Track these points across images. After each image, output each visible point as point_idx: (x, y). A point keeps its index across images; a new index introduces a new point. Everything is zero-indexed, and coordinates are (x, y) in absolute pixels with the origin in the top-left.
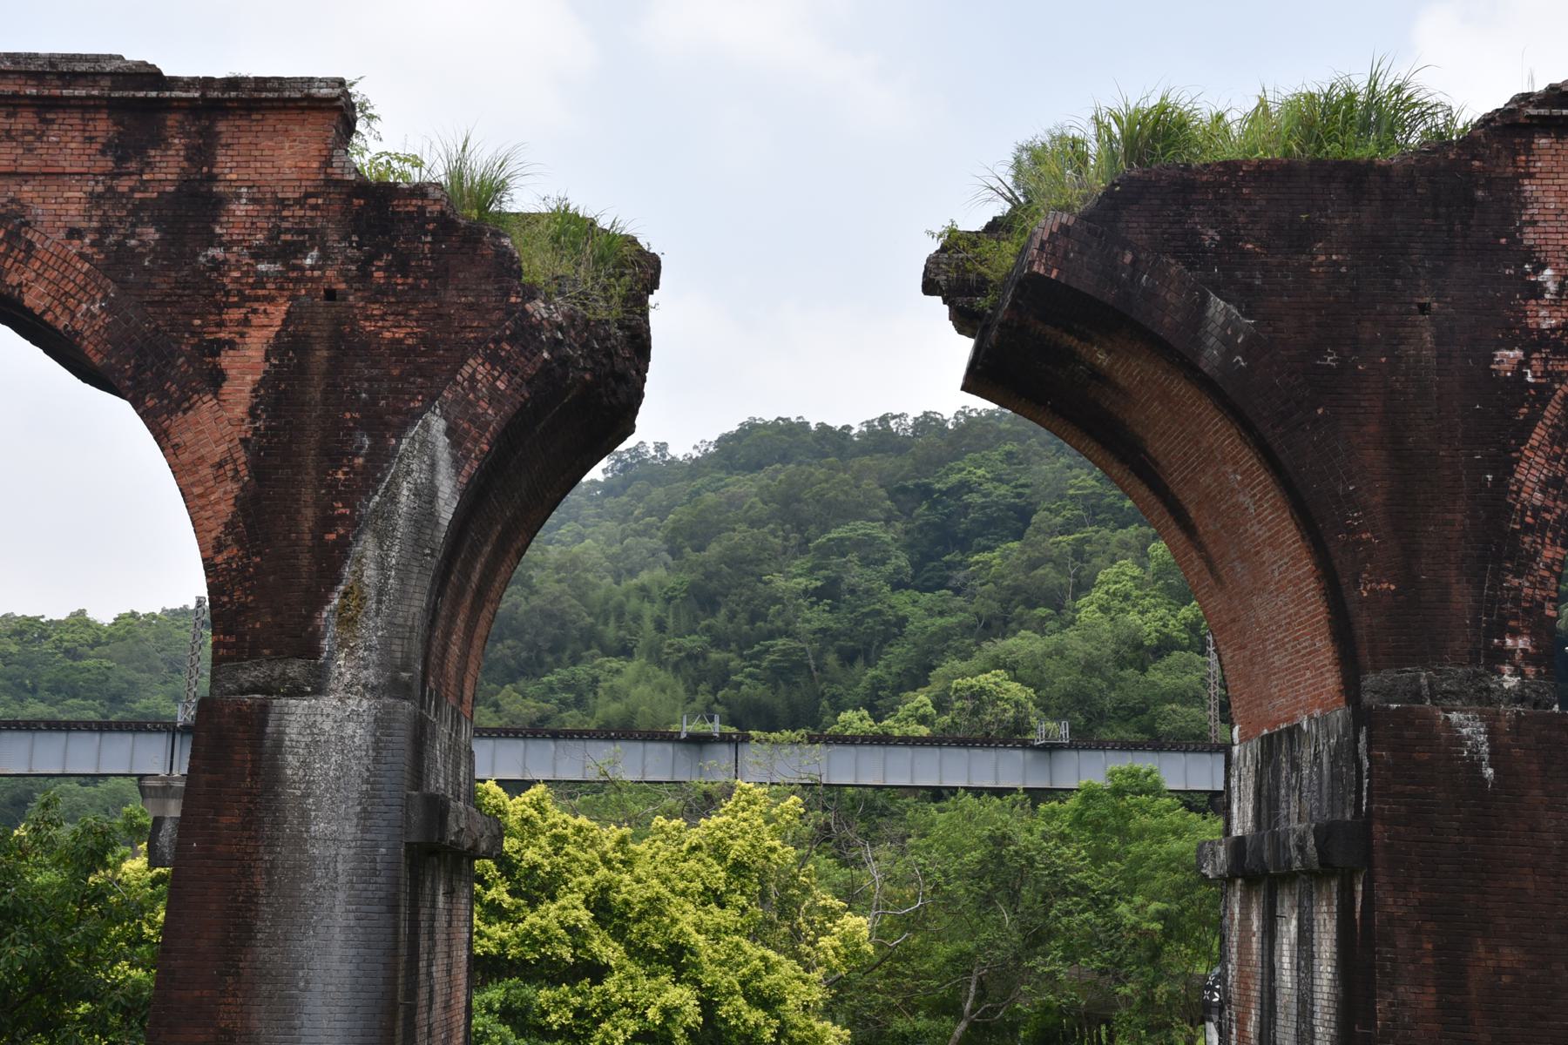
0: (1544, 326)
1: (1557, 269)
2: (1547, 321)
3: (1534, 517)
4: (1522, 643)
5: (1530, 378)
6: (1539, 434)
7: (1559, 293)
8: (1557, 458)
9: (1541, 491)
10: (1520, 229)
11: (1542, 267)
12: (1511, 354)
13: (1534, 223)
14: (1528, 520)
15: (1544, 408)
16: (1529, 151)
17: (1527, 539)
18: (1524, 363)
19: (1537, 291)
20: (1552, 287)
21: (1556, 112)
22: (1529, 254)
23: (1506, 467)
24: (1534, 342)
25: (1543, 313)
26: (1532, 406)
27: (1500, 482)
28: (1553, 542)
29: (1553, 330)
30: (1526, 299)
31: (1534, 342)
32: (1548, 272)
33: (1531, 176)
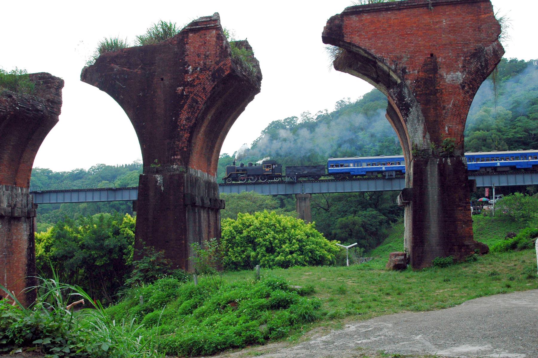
0: (189, 80)
1: (192, 66)
2: (190, 79)
3: (183, 127)
4: (179, 157)
5: (185, 94)
6: (186, 107)
7: (192, 72)
8: (189, 112)
9: (185, 121)
10: (184, 57)
11: (189, 66)
12: (180, 88)
13: (187, 55)
14: (182, 128)
15: (187, 101)
16: (187, 37)
17: (181, 133)
18: (183, 90)
19: (187, 72)
20: (191, 70)
21: (192, 28)
22: (186, 63)
23: (177, 115)
24: (186, 84)
25: (189, 77)
26: (185, 100)
27: (176, 119)
28: (187, 132)
29: (191, 81)
30: (185, 74)
31: (186, 84)
32: (190, 67)
33: (187, 43)
